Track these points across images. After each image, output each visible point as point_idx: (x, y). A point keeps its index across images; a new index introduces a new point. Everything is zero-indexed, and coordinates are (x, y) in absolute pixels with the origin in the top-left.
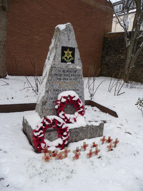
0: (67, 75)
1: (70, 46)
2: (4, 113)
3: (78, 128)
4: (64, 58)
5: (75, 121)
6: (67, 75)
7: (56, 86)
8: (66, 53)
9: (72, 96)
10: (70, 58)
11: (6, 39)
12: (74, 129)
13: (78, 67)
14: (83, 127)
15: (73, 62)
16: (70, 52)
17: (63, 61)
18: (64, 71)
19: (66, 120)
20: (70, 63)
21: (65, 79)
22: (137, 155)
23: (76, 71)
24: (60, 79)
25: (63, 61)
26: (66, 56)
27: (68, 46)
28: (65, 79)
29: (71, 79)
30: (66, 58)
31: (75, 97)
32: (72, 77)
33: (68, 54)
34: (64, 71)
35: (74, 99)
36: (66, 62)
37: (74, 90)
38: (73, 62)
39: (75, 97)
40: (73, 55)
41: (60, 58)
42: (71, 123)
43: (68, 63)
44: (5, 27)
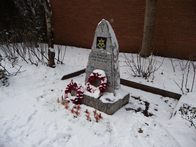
0: (100, 58)
1: (103, 37)
2: (142, 90)
3: (91, 97)
4: (98, 45)
5: (94, 92)
6: (100, 58)
7: (93, 65)
8: (100, 41)
9: (99, 74)
10: (103, 45)
11: (152, 24)
12: (88, 96)
13: (108, 53)
14: (94, 98)
15: (105, 48)
16: (103, 41)
17: (97, 47)
18: (98, 55)
19: (89, 89)
20: (102, 49)
21: (98, 61)
22: (37, 100)
23: (106, 56)
24: (95, 60)
25: (97, 47)
26: (100, 44)
27: (102, 37)
28: (98, 61)
29: (102, 61)
30: (100, 45)
31: (100, 75)
32: (103, 60)
33: (101, 42)
34: (98, 55)
35: (99, 76)
36: (100, 48)
37: (104, 70)
38: (105, 48)
39: (100, 75)
40: (105, 43)
41: (96, 45)
42: (91, 92)
43: (101, 49)
44: (152, 14)
